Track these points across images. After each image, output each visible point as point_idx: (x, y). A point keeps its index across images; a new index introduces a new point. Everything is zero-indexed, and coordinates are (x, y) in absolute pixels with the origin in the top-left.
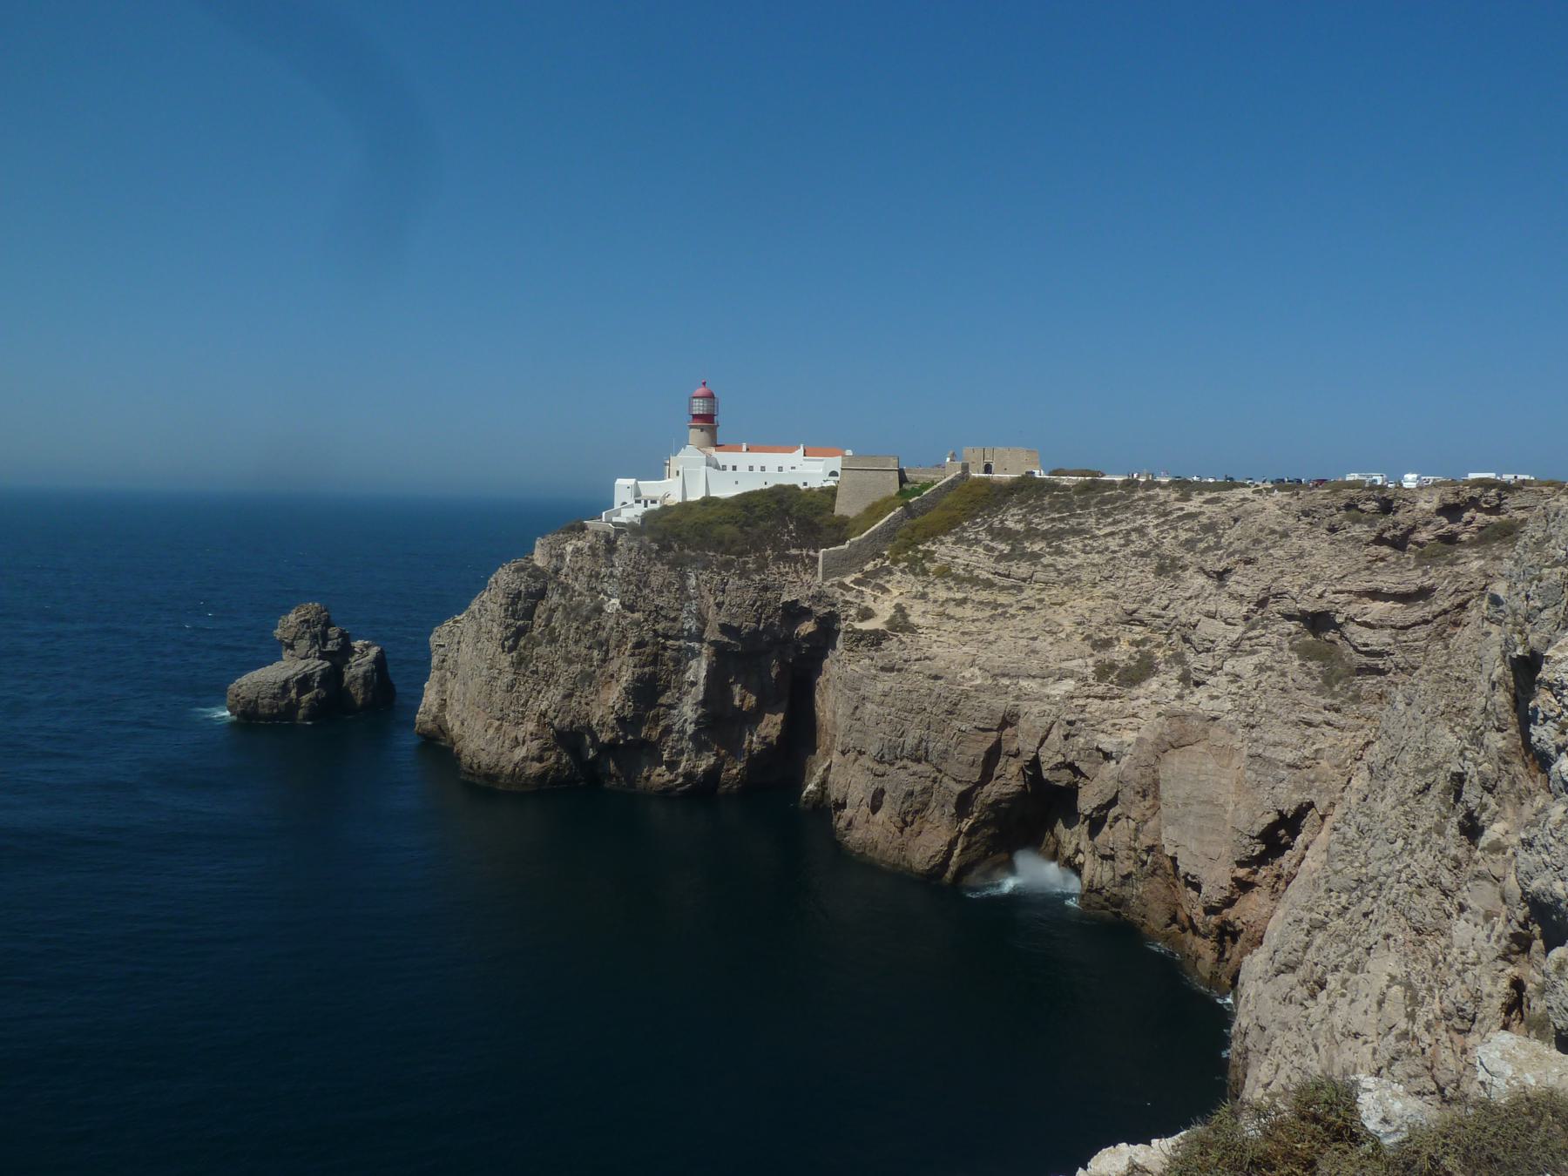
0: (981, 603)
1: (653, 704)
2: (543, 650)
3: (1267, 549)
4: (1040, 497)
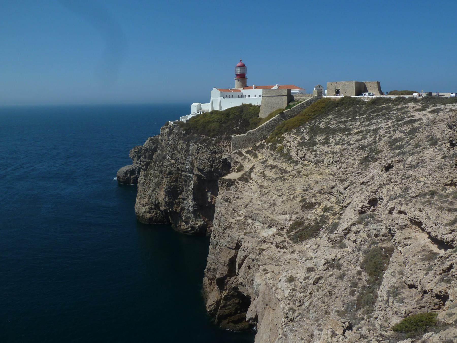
0: (280, 169)
1: (176, 197)
2: (152, 172)
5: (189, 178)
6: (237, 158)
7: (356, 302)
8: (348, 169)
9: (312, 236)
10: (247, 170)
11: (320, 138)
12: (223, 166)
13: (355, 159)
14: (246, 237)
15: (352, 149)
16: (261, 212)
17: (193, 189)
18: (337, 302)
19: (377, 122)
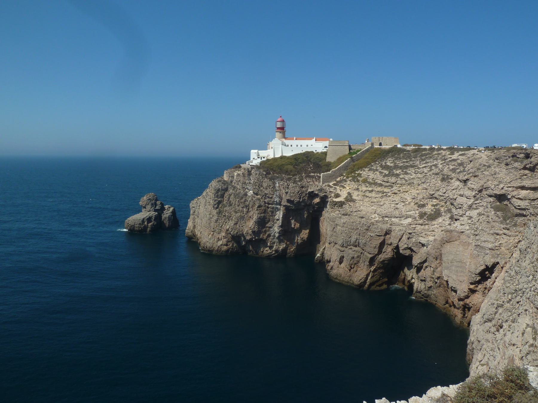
0: (378, 191)
3: (482, 172)
4: (399, 154)
9: (439, 217)
12: (308, 197)
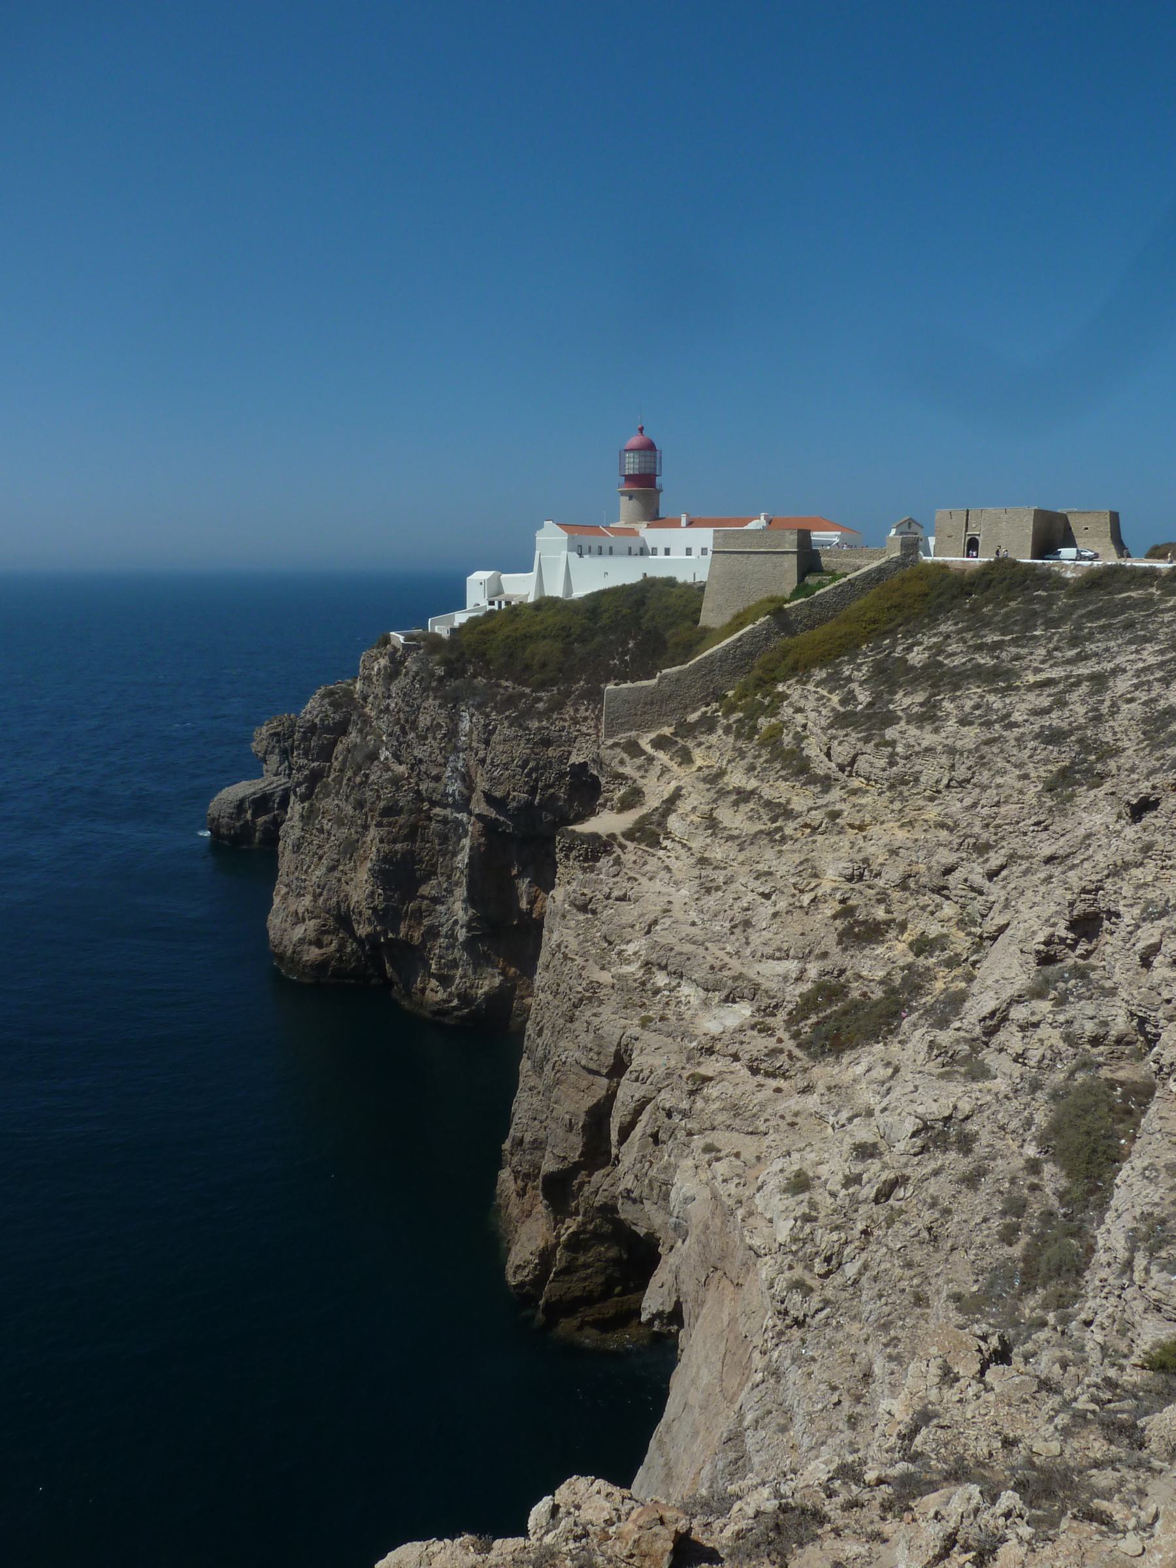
0: (769, 804)
1: (410, 893)
2: (328, 804)
5: (456, 829)
6: (622, 762)
7: (1021, 1265)
8: (1003, 810)
9: (872, 1036)
10: (657, 804)
11: (907, 701)
12: (573, 790)
13: (1026, 777)
14: (646, 1036)
15: (1016, 739)
16: (701, 951)
17: (470, 865)
18: (954, 1263)
19: (1107, 650)
